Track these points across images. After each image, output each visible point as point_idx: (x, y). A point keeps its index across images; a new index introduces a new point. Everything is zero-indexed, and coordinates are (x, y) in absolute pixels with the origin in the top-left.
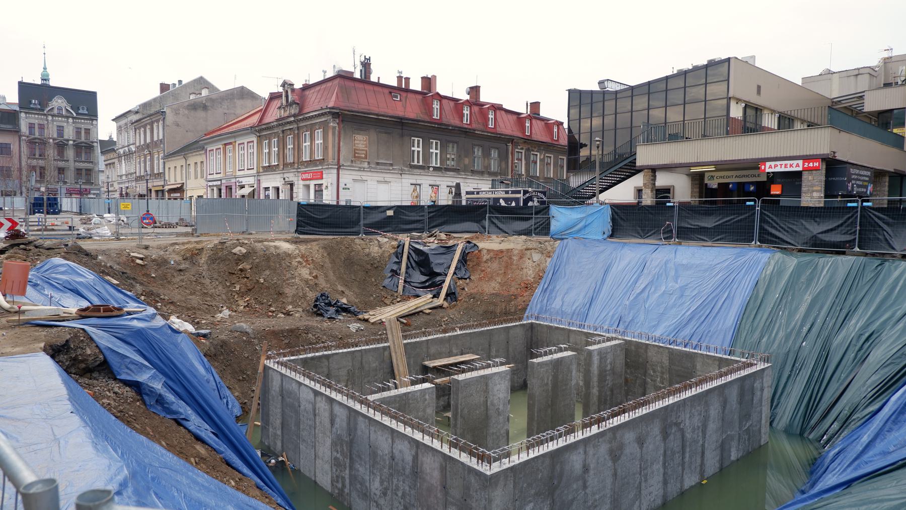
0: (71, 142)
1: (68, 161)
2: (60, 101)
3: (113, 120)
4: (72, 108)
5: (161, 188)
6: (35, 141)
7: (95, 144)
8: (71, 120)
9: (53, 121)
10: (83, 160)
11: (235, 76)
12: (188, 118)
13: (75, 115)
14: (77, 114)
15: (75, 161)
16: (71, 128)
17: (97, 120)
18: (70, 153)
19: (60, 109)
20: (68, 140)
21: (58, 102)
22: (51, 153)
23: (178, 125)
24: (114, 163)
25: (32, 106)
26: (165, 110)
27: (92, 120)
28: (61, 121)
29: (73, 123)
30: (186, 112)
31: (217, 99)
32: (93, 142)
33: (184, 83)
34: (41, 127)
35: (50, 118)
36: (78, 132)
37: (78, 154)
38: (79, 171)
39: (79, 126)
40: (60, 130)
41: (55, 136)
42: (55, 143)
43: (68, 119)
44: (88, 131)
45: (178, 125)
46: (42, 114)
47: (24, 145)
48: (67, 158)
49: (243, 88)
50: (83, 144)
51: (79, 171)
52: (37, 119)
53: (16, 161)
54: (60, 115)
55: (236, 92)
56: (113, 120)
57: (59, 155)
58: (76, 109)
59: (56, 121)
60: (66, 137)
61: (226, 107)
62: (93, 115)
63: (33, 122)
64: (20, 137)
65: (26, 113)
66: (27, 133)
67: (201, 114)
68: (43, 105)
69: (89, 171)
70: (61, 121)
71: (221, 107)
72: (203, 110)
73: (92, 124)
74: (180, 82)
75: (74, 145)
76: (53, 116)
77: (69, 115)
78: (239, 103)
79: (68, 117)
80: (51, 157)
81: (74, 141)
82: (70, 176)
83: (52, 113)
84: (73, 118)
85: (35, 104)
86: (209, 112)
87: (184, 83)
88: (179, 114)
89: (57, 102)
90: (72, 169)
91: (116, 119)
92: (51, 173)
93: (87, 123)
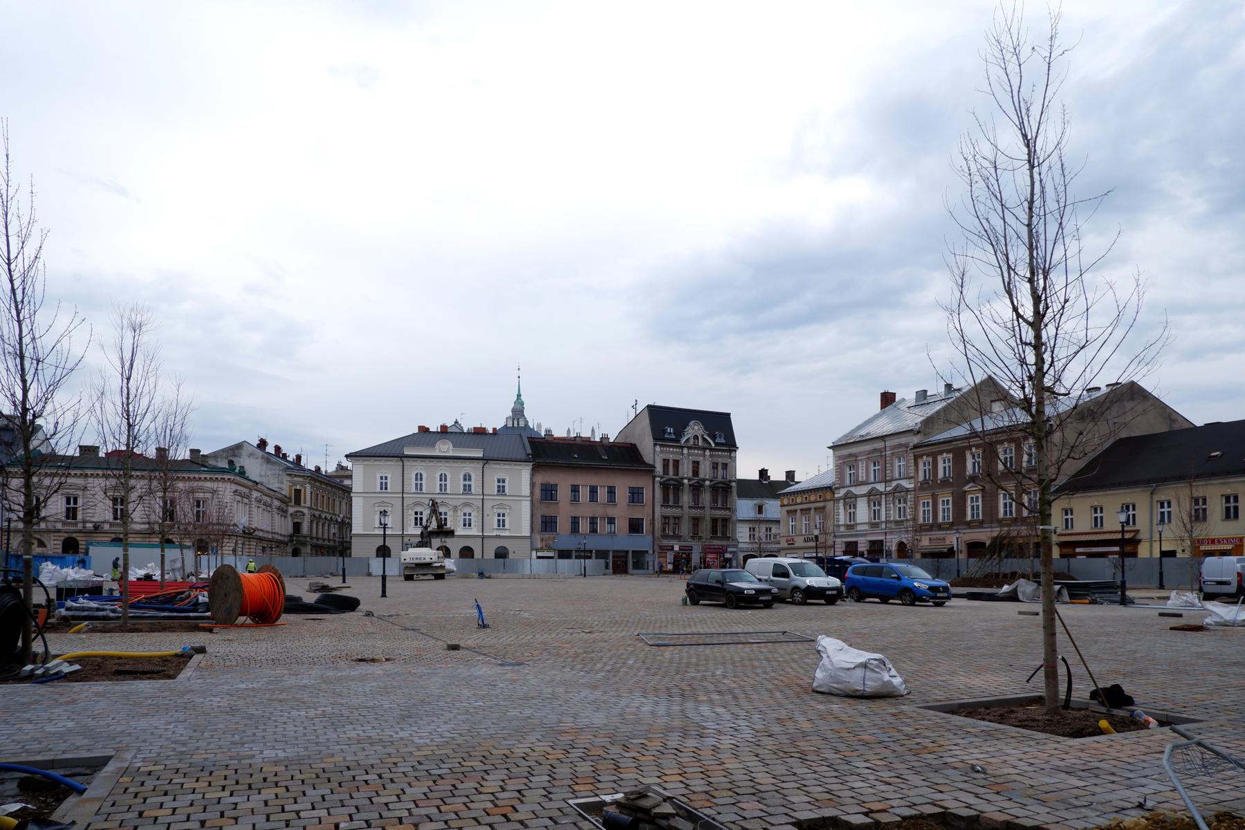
0: (707, 483)
1: (703, 508)
2: (696, 428)
3: (830, 448)
4: (708, 435)
6: (668, 482)
7: (734, 484)
8: (708, 453)
9: (689, 454)
10: (719, 505)
13: (713, 445)
14: (717, 444)
15: (711, 508)
16: (708, 463)
17: (735, 451)
18: (706, 498)
19: (696, 437)
20: (704, 480)
21: (695, 429)
22: (686, 498)
24: (824, 508)
25: (666, 436)
27: (731, 451)
28: (697, 455)
29: (711, 456)
32: (730, 481)
34: (676, 463)
35: (685, 451)
36: (715, 466)
37: (715, 500)
38: (714, 521)
39: (716, 460)
40: (696, 464)
41: (690, 475)
42: (690, 485)
43: (704, 452)
44: (725, 466)
46: (676, 447)
47: (657, 486)
48: (703, 503)
50: (720, 485)
51: (714, 521)
52: (673, 453)
53: (648, 510)
54: (696, 447)
56: (830, 448)
57: (694, 501)
58: (714, 438)
59: (692, 455)
60: (702, 476)
62: (730, 445)
63: (667, 458)
64: (654, 477)
65: (661, 445)
66: (661, 474)
68: (679, 434)
69: (725, 521)
70: (697, 455)
73: (730, 457)
75: (710, 486)
76: (689, 448)
77: (706, 446)
79: (704, 449)
80: (686, 506)
81: (711, 481)
82: (706, 528)
83: (689, 445)
84: (711, 450)
85: (670, 433)
89: (693, 429)
90: (708, 518)
91: (834, 447)
92: (685, 529)
93: (725, 456)
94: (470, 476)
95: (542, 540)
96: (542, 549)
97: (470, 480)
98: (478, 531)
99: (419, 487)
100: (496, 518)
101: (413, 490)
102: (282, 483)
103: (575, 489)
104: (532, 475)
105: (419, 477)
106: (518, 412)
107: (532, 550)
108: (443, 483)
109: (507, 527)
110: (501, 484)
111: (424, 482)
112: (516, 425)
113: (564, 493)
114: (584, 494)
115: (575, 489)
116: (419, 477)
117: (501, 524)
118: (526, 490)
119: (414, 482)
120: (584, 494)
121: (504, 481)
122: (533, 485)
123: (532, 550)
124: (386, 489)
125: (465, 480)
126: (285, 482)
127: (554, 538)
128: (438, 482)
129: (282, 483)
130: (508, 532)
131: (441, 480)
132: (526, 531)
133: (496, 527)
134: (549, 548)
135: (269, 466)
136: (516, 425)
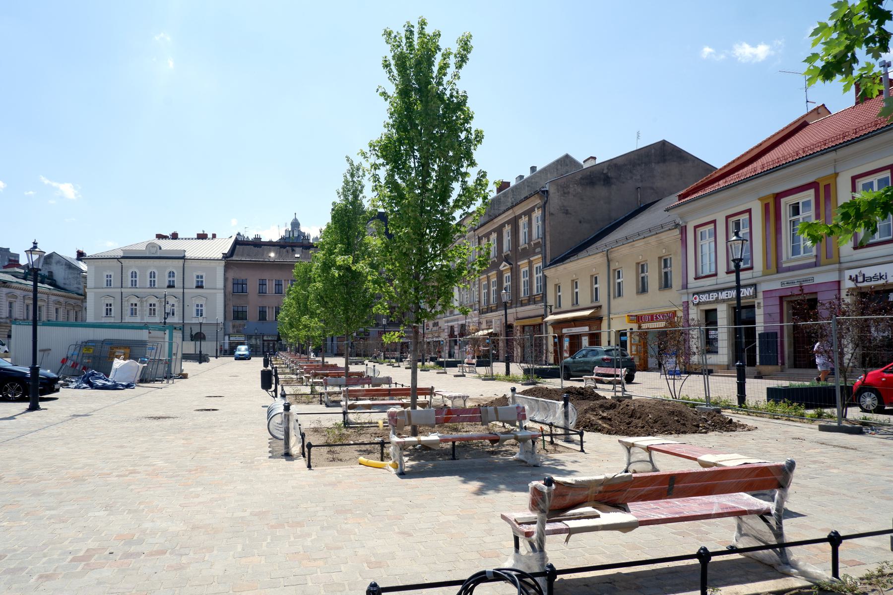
5: (538, 321)
11: (638, 133)
12: (582, 199)
23: (567, 212)
26: (547, 189)
30: (579, 189)
31: (625, 165)
33: (538, 169)
45: (567, 212)
49: (664, 143)
55: (653, 151)
61: (638, 177)
67: (601, 191)
71: (631, 178)
72: (604, 185)
74: (533, 169)
78: (659, 168)
86: (614, 187)
87: (538, 169)
88: (569, 193)
94: (173, 273)
95: (234, 327)
96: (234, 334)
97: (173, 276)
98: (179, 320)
99: (134, 284)
100: (195, 308)
101: (130, 285)
102: (79, 284)
103: (262, 283)
104: (225, 271)
105: (134, 275)
106: (295, 224)
107: (225, 335)
108: (152, 279)
109: (204, 315)
110: (200, 279)
111: (137, 279)
112: (291, 236)
113: (252, 286)
114: (270, 287)
115: (262, 283)
116: (134, 275)
117: (199, 313)
118: (220, 283)
119: (130, 279)
120: (270, 287)
121: (202, 277)
122: (226, 279)
123: (225, 335)
124: (110, 285)
125: (170, 276)
126: (81, 283)
127: (244, 325)
128: (149, 279)
129: (79, 284)
130: (113, 318)
131: (151, 277)
132: (220, 318)
133: (195, 315)
134: (238, 332)
135: (71, 271)
136: (291, 236)
